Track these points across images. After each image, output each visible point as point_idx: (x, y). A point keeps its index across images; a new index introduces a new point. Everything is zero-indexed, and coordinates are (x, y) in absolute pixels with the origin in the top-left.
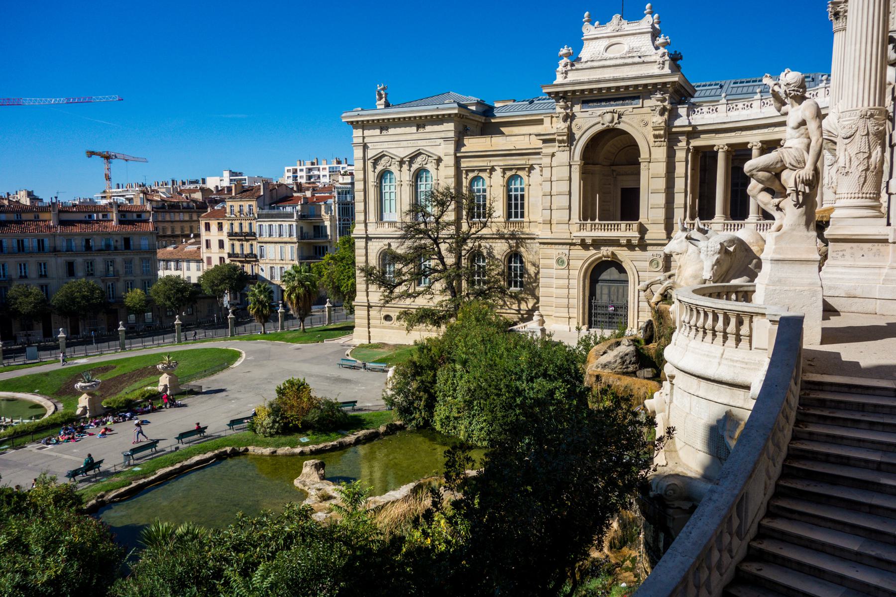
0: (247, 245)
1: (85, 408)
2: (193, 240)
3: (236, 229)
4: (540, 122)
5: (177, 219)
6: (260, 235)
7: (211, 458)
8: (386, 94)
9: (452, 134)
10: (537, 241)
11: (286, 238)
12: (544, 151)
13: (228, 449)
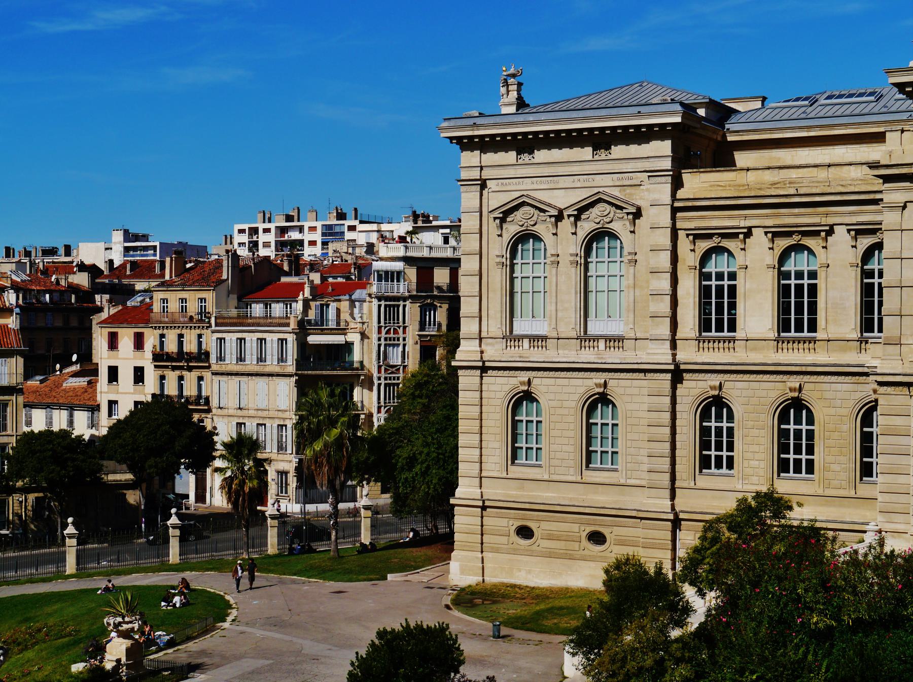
0: (190, 378)
2: (75, 368)
3: (171, 346)
4: (879, 138)
5: (41, 324)
6: (221, 358)
8: (520, 85)
9: (667, 164)
10: (872, 378)
11: (271, 364)
12: (887, 198)
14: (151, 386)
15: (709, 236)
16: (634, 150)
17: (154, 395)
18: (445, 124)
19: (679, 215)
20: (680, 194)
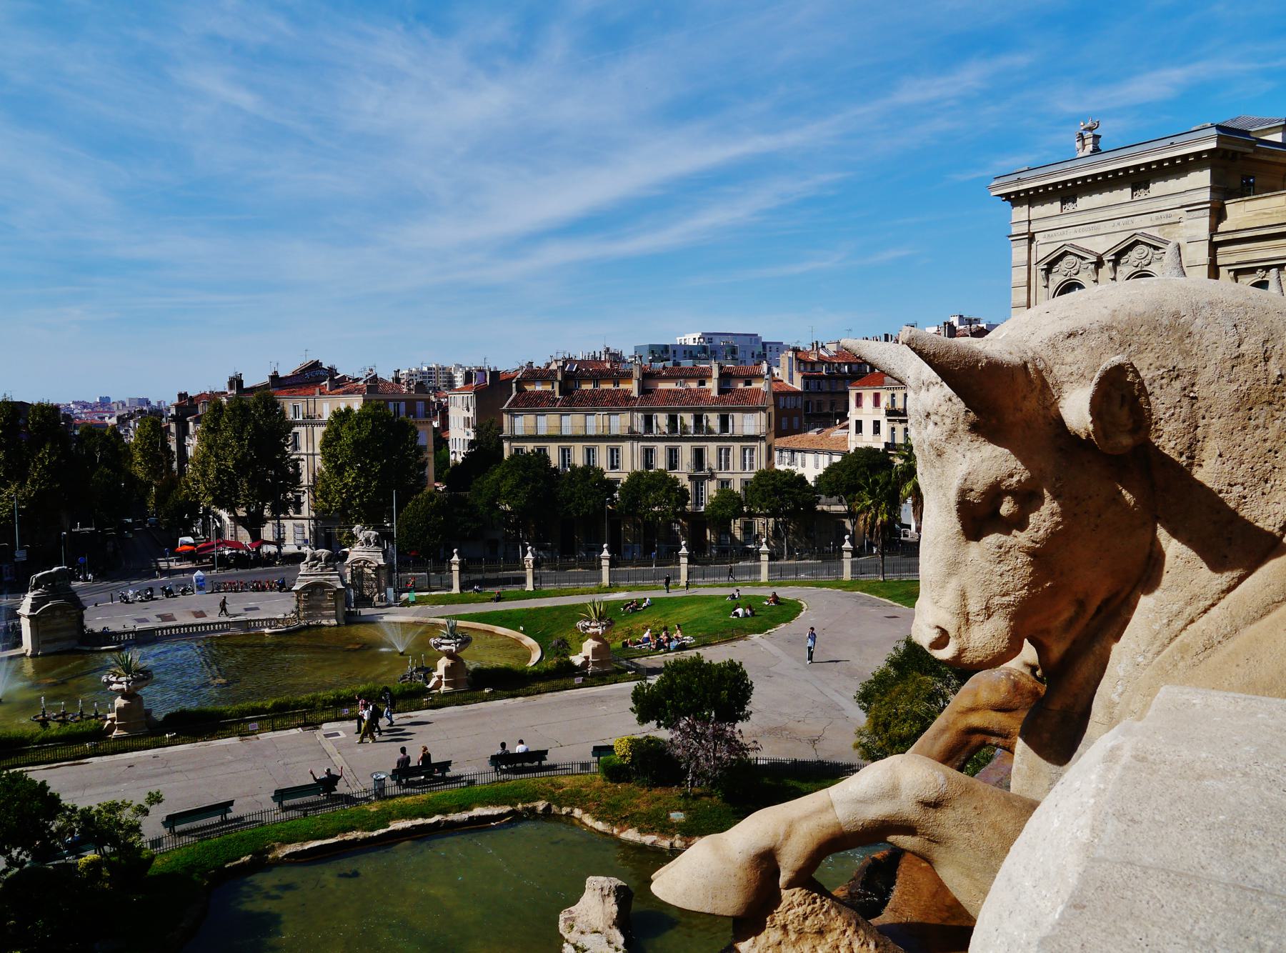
1: (440, 677)
7: (501, 816)
8: (1096, 137)
9: (1206, 195)
13: (541, 805)
14: (885, 436)
15: (1252, 271)
16: (1173, 185)
17: (886, 444)
18: (995, 183)
19: (1220, 250)
20: (1222, 227)
